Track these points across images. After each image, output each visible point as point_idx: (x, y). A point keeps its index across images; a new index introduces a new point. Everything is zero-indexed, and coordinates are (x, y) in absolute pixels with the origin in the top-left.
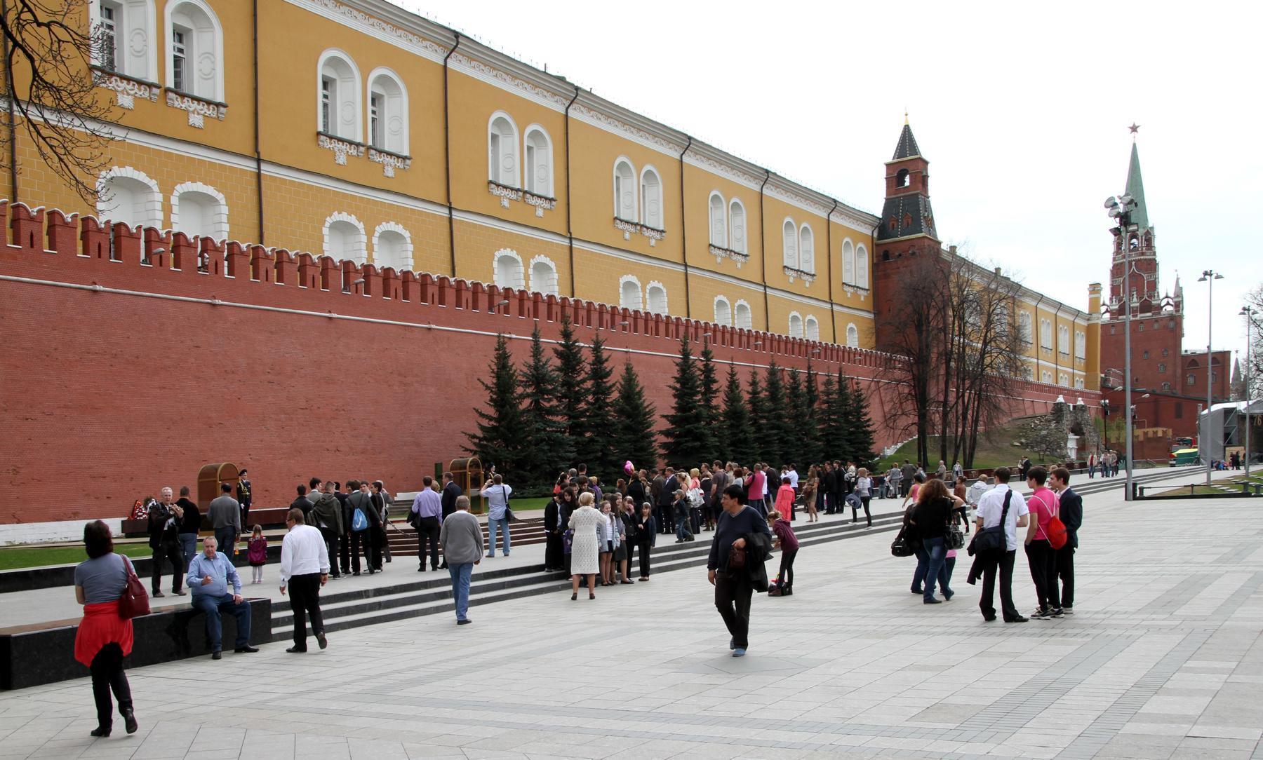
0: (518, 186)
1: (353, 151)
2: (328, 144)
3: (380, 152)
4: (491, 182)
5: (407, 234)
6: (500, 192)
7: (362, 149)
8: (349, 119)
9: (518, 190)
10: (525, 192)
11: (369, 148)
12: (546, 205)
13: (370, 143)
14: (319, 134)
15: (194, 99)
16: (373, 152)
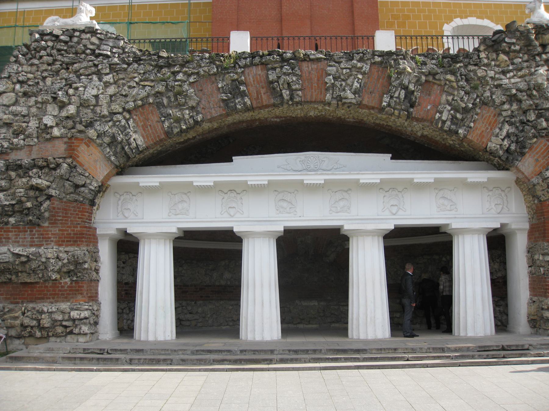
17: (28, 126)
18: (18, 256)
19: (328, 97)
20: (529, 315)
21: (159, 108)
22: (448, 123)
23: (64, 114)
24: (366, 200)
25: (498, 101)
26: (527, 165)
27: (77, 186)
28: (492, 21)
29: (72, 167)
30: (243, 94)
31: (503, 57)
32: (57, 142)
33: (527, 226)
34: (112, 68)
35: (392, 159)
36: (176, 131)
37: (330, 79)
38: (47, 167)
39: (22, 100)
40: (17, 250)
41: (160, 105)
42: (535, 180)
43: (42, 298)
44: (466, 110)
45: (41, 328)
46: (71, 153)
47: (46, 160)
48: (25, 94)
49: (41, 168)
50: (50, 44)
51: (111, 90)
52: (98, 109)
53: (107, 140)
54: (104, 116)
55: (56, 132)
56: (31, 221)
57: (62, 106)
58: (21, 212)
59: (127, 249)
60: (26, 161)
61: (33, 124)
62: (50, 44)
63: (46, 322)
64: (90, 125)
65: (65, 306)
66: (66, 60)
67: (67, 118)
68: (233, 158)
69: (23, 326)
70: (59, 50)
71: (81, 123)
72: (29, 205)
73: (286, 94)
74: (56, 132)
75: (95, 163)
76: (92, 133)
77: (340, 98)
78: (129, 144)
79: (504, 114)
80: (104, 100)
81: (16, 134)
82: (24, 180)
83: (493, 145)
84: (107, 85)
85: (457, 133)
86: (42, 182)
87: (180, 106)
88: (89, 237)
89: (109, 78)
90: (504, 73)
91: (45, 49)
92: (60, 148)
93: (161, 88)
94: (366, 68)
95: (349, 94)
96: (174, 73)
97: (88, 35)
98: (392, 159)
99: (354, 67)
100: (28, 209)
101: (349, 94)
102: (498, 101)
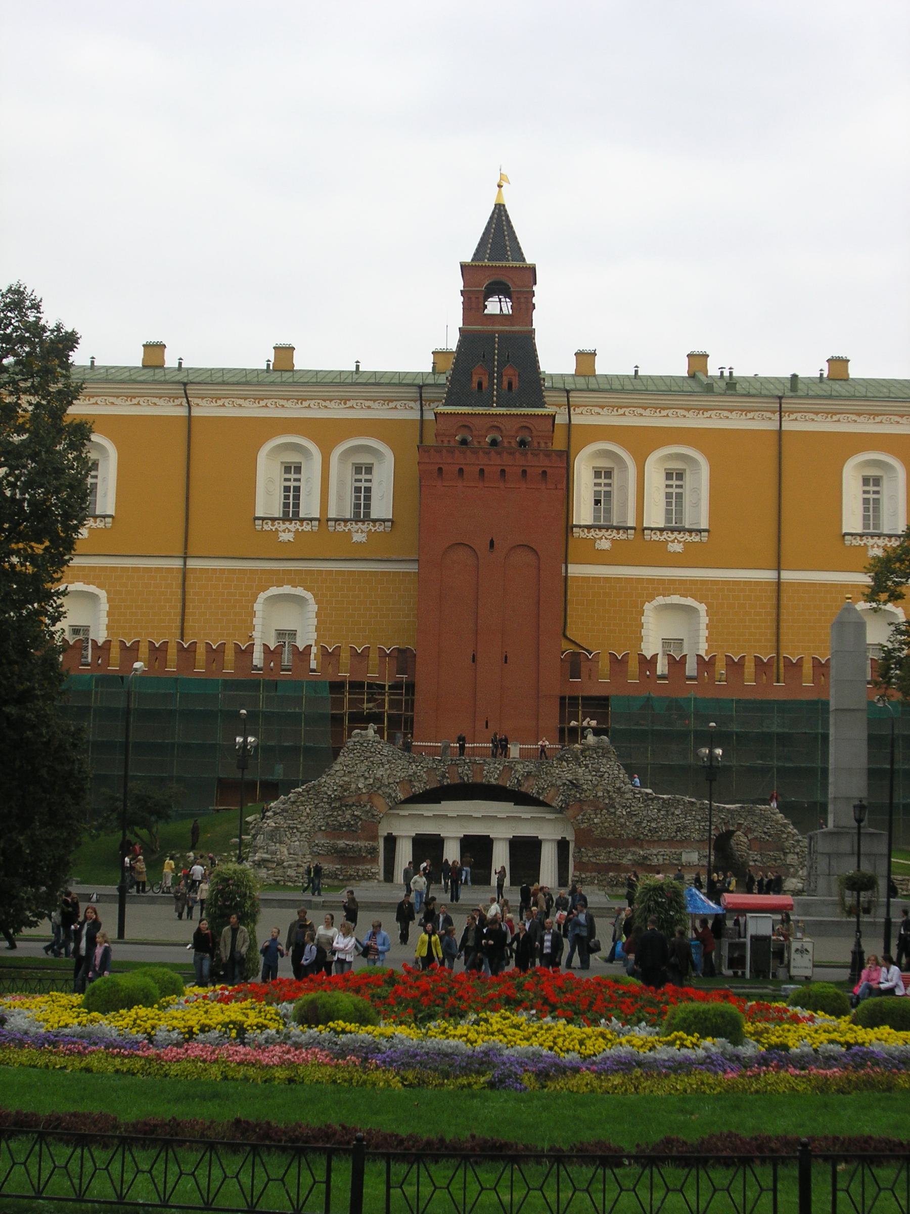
24: (501, 824)
26: (570, 813)
27: (373, 815)
28: (696, 600)
29: (371, 807)
31: (564, 763)
34: (389, 761)
40: (347, 843)
41: (411, 781)
43: (359, 864)
44: (543, 788)
45: (358, 876)
46: (370, 800)
51: (388, 772)
55: (364, 791)
57: (366, 778)
59: (391, 841)
61: (353, 786)
63: (360, 873)
64: (379, 788)
65: (368, 867)
69: (351, 875)
73: (466, 779)
75: (380, 804)
76: (380, 792)
81: (345, 791)
83: (554, 804)
84: (387, 770)
88: (375, 838)
89: (387, 766)
92: (365, 798)
94: (501, 768)
95: (492, 780)
96: (417, 766)
99: (496, 768)
101: (492, 780)
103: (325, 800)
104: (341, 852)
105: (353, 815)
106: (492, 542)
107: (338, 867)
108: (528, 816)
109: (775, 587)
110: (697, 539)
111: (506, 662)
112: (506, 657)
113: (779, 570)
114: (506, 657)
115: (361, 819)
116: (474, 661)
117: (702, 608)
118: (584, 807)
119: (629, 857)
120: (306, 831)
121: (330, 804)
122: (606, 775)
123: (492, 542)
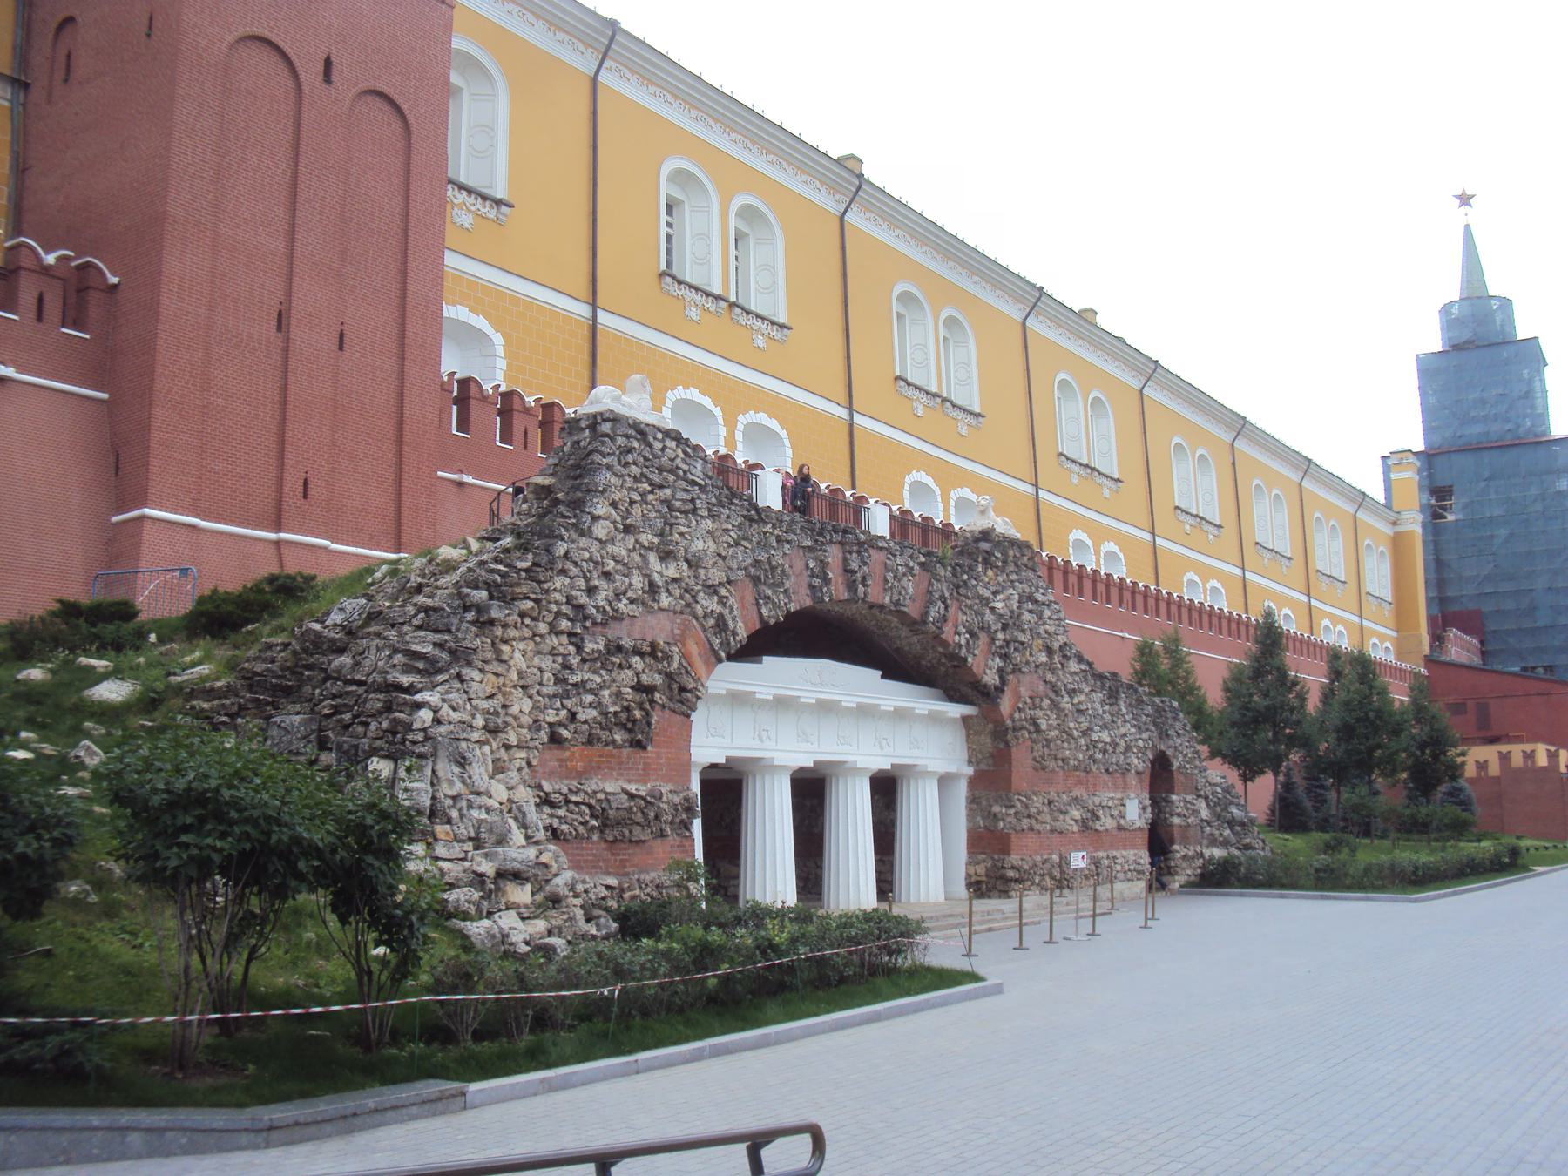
0: (934, 389)
1: (710, 304)
2: (675, 289)
3: (748, 313)
4: (897, 378)
5: (784, 434)
6: (910, 392)
7: (723, 304)
8: (704, 262)
9: (935, 395)
10: (944, 400)
11: (732, 305)
12: (973, 421)
13: (733, 298)
14: (662, 275)
15: (461, 187)
16: (738, 311)
17: (631, 584)
18: (632, 796)
19: (887, 599)
20: (968, 876)
21: (755, 585)
22: (964, 650)
23: (672, 572)
25: (994, 628)
30: (826, 581)
31: (990, 573)
32: (662, 615)
33: (970, 771)
35: (883, 677)
36: (772, 621)
37: (890, 576)
38: (653, 652)
39: (620, 536)
40: (632, 788)
42: (1009, 723)
47: (653, 645)
48: (628, 529)
49: (642, 654)
50: (636, 445)
52: (702, 572)
53: (711, 622)
54: (710, 587)
56: (639, 741)
58: (624, 726)
60: (627, 643)
61: (638, 581)
62: (636, 445)
66: (656, 478)
67: (674, 580)
68: (765, 658)
70: (646, 459)
71: (686, 591)
72: (638, 714)
74: (665, 601)
77: (897, 603)
78: (734, 634)
79: (998, 643)
80: (708, 562)
82: (630, 673)
85: (965, 659)
86: (652, 678)
87: (774, 586)
90: (995, 593)
91: (630, 451)
93: (763, 557)
97: (674, 444)
98: (883, 677)
100: (634, 721)
102: (994, 628)
103: (565, 624)
104: (618, 823)
105: (639, 687)
106: (328, 63)
107: (613, 881)
108: (887, 704)
109: (586, 333)
110: (492, 214)
111: (341, 348)
112: (341, 335)
113: (594, 305)
114: (341, 335)
115: (652, 701)
116: (279, 329)
117: (498, 339)
118: (1023, 690)
119: (1076, 814)
120: (518, 746)
121: (577, 641)
122: (1047, 613)
123: (328, 63)
